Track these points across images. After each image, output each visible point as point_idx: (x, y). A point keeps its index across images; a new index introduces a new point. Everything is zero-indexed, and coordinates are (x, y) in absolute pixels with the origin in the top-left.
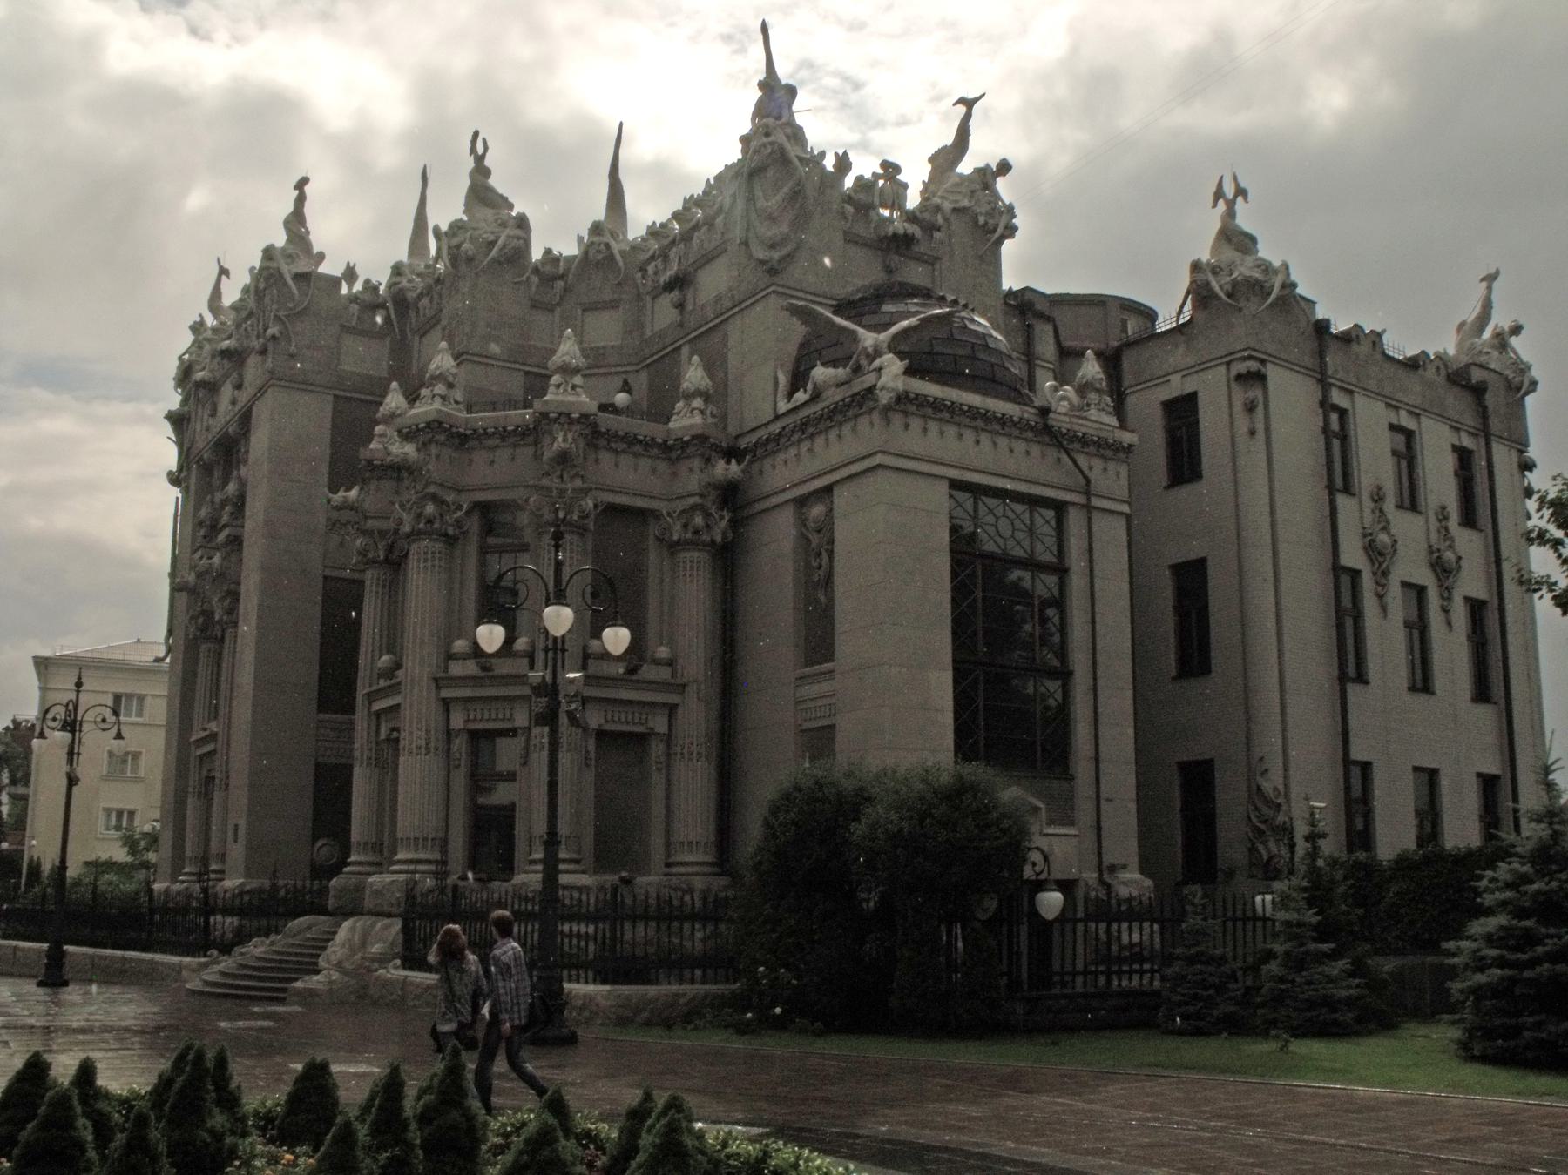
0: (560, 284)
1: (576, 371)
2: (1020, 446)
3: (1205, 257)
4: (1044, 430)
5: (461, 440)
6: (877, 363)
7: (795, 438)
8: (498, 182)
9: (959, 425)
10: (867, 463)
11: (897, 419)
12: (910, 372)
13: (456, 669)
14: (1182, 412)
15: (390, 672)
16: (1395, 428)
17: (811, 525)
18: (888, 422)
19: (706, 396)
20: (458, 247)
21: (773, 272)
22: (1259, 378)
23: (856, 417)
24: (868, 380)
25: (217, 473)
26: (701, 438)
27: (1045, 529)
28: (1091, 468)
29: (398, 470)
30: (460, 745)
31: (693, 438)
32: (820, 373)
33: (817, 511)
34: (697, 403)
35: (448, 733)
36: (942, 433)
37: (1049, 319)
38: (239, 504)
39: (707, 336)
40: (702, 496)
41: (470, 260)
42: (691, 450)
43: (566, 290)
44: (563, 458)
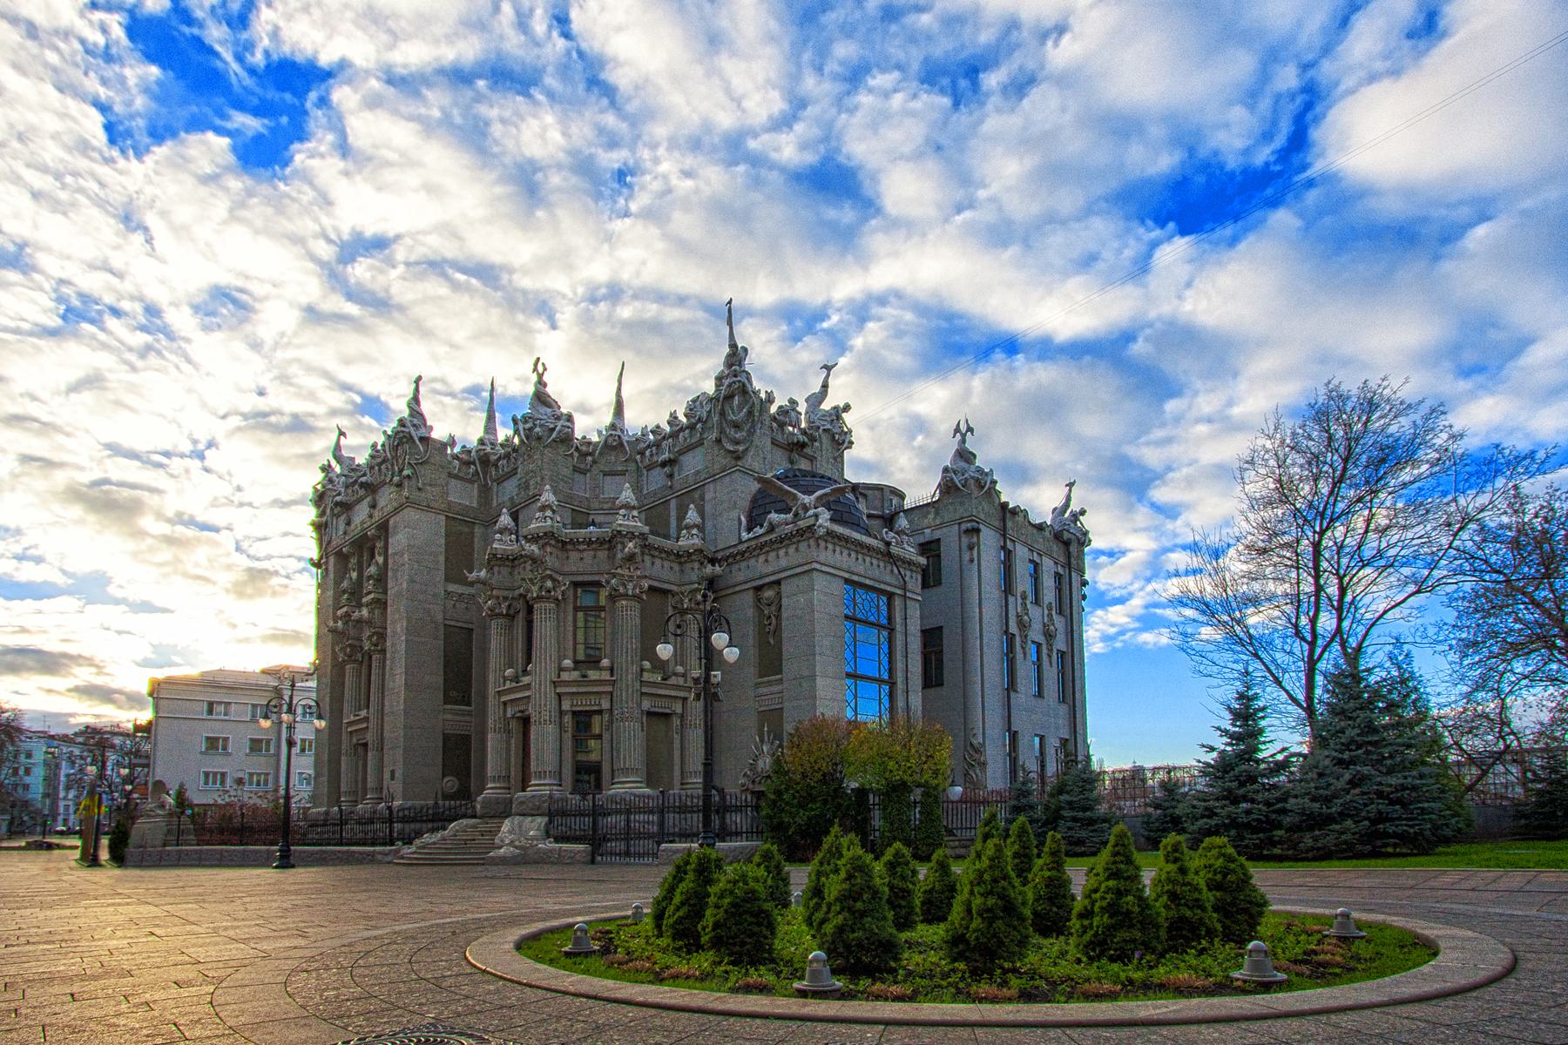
0: (590, 458)
1: (634, 508)
2: (875, 562)
4: (888, 556)
5: (564, 545)
6: (811, 512)
10: (806, 568)
11: (822, 544)
12: (831, 520)
13: (565, 676)
14: (930, 548)
15: (516, 679)
16: (1031, 561)
19: (696, 526)
20: (530, 429)
21: (738, 458)
22: (977, 531)
24: (812, 521)
25: (353, 560)
27: (884, 608)
29: (512, 561)
30: (568, 719)
32: (774, 516)
33: (769, 593)
34: (695, 531)
35: (561, 713)
37: (865, 496)
38: (381, 580)
39: (693, 494)
41: (539, 438)
43: (594, 462)
44: (631, 558)
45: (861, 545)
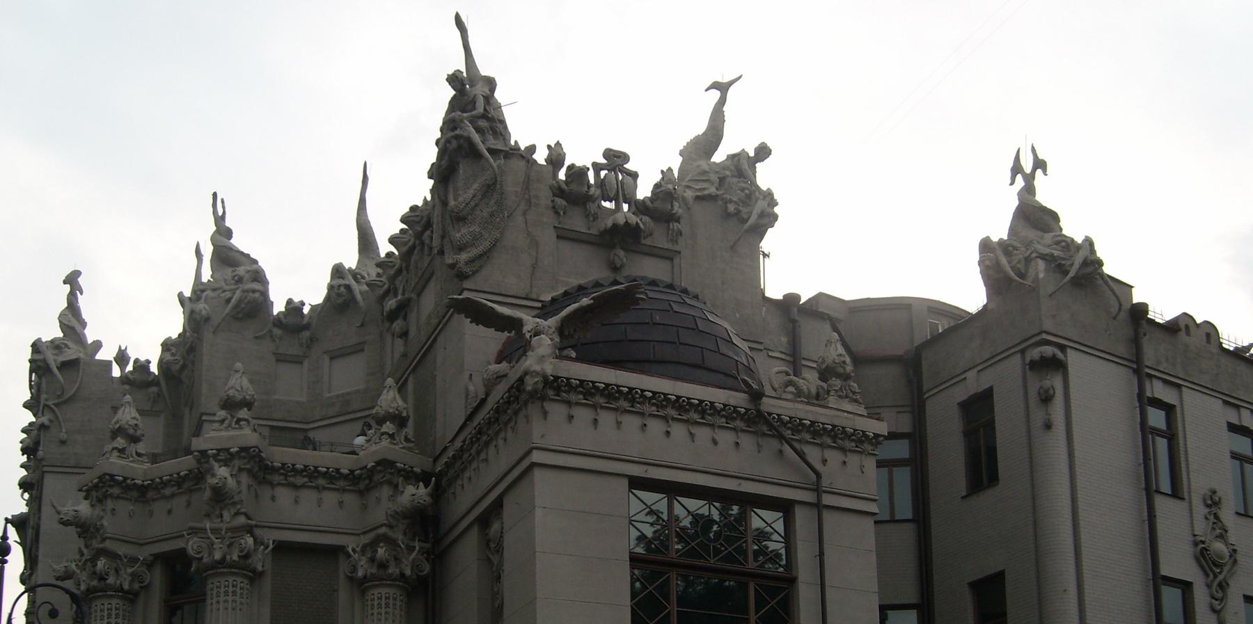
2: (726, 438)
3: (1000, 231)
4: (756, 421)
7: (473, 451)
8: (240, 242)
9: (642, 414)
11: (557, 411)
17: (492, 545)
18: (545, 414)
23: (516, 413)
26: (385, 463)
28: (824, 461)
31: (378, 463)
33: (496, 526)
36: (619, 424)
40: (391, 527)
41: (207, 319)
42: (377, 477)
45: (682, 405)
